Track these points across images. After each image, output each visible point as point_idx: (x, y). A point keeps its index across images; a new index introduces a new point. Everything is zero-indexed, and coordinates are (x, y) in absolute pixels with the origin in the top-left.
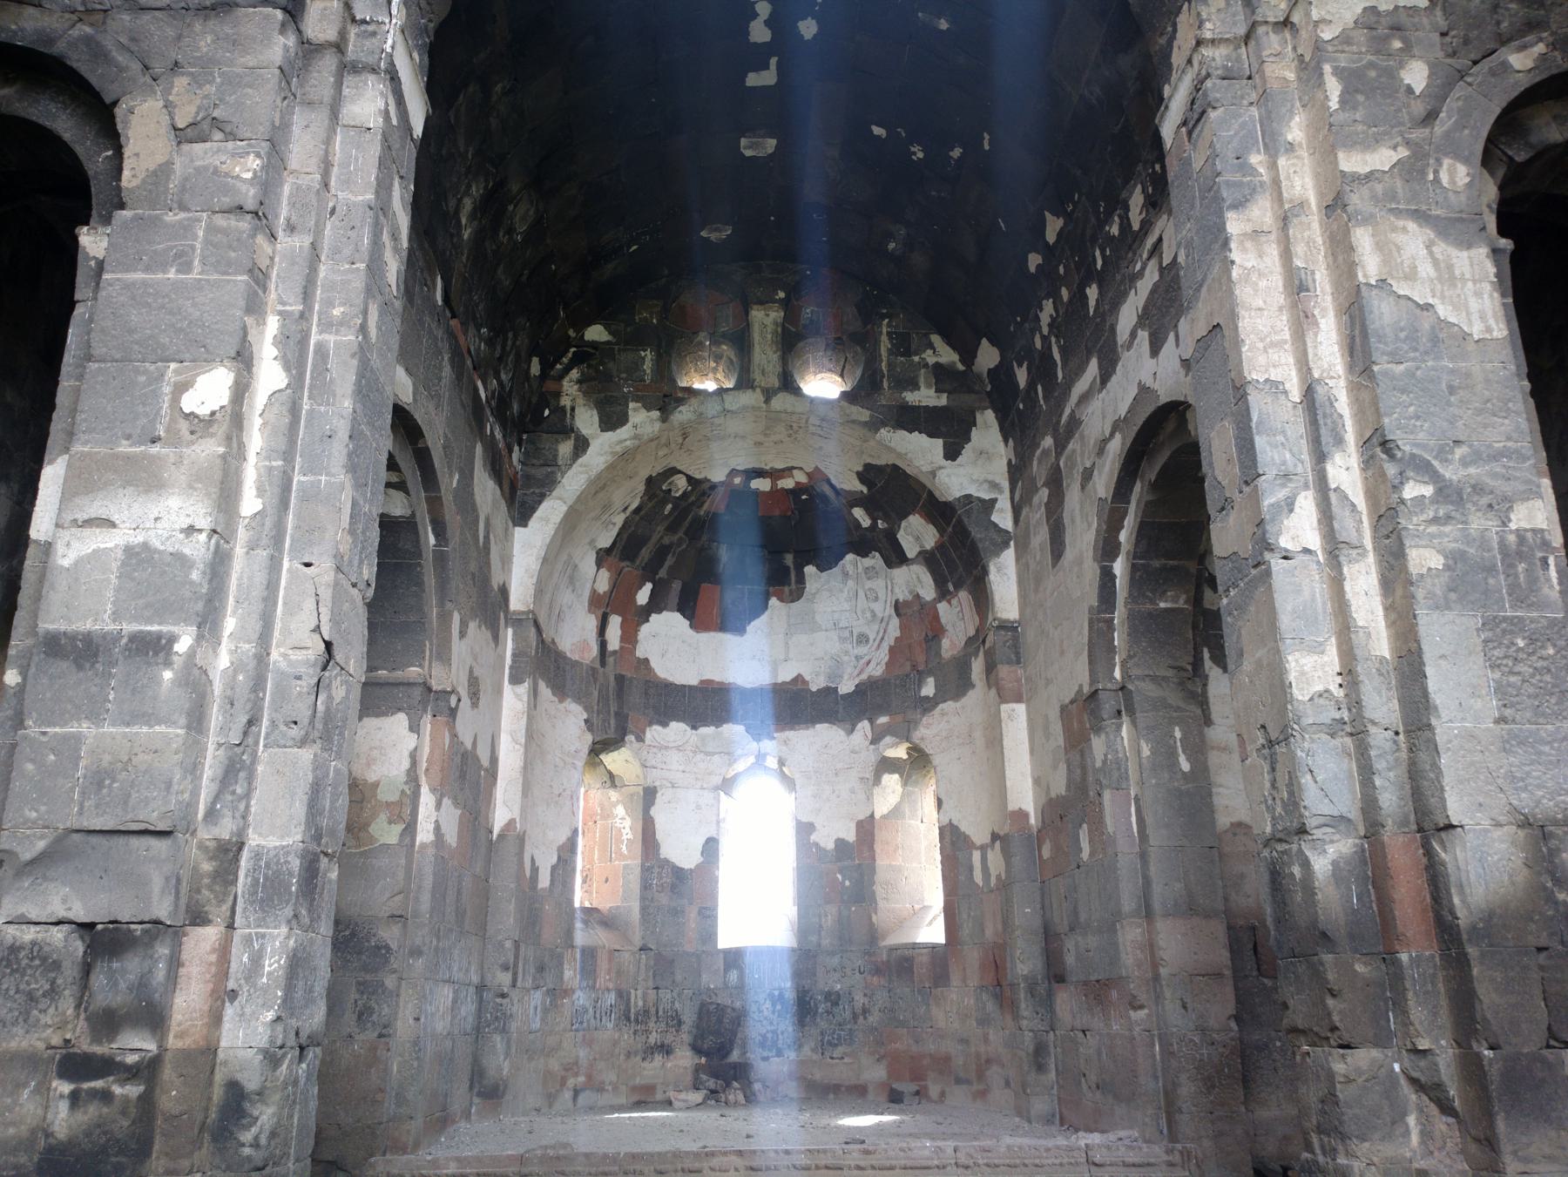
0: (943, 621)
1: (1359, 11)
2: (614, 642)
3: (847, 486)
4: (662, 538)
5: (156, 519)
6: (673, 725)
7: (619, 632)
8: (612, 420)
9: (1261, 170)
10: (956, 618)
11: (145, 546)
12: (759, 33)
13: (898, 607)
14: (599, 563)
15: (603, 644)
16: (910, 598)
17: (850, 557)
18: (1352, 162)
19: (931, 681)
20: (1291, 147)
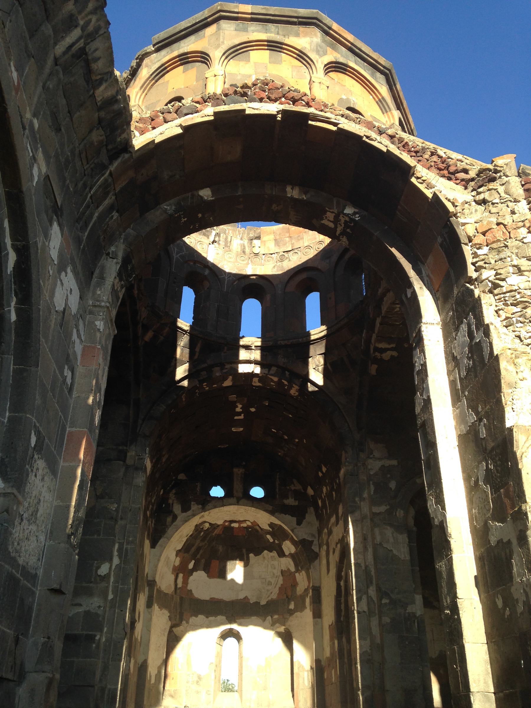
0: (297, 580)
1: (380, 466)
2: (180, 585)
3: (265, 528)
4: (199, 544)
5: (92, 604)
6: (200, 616)
7: (182, 580)
8: (185, 508)
9: (359, 503)
10: (301, 578)
11: (89, 611)
12: (238, 409)
13: (282, 572)
14: (177, 556)
15: (176, 585)
16: (286, 570)
17: (266, 552)
18: (376, 510)
19: (293, 603)
20: (364, 499)
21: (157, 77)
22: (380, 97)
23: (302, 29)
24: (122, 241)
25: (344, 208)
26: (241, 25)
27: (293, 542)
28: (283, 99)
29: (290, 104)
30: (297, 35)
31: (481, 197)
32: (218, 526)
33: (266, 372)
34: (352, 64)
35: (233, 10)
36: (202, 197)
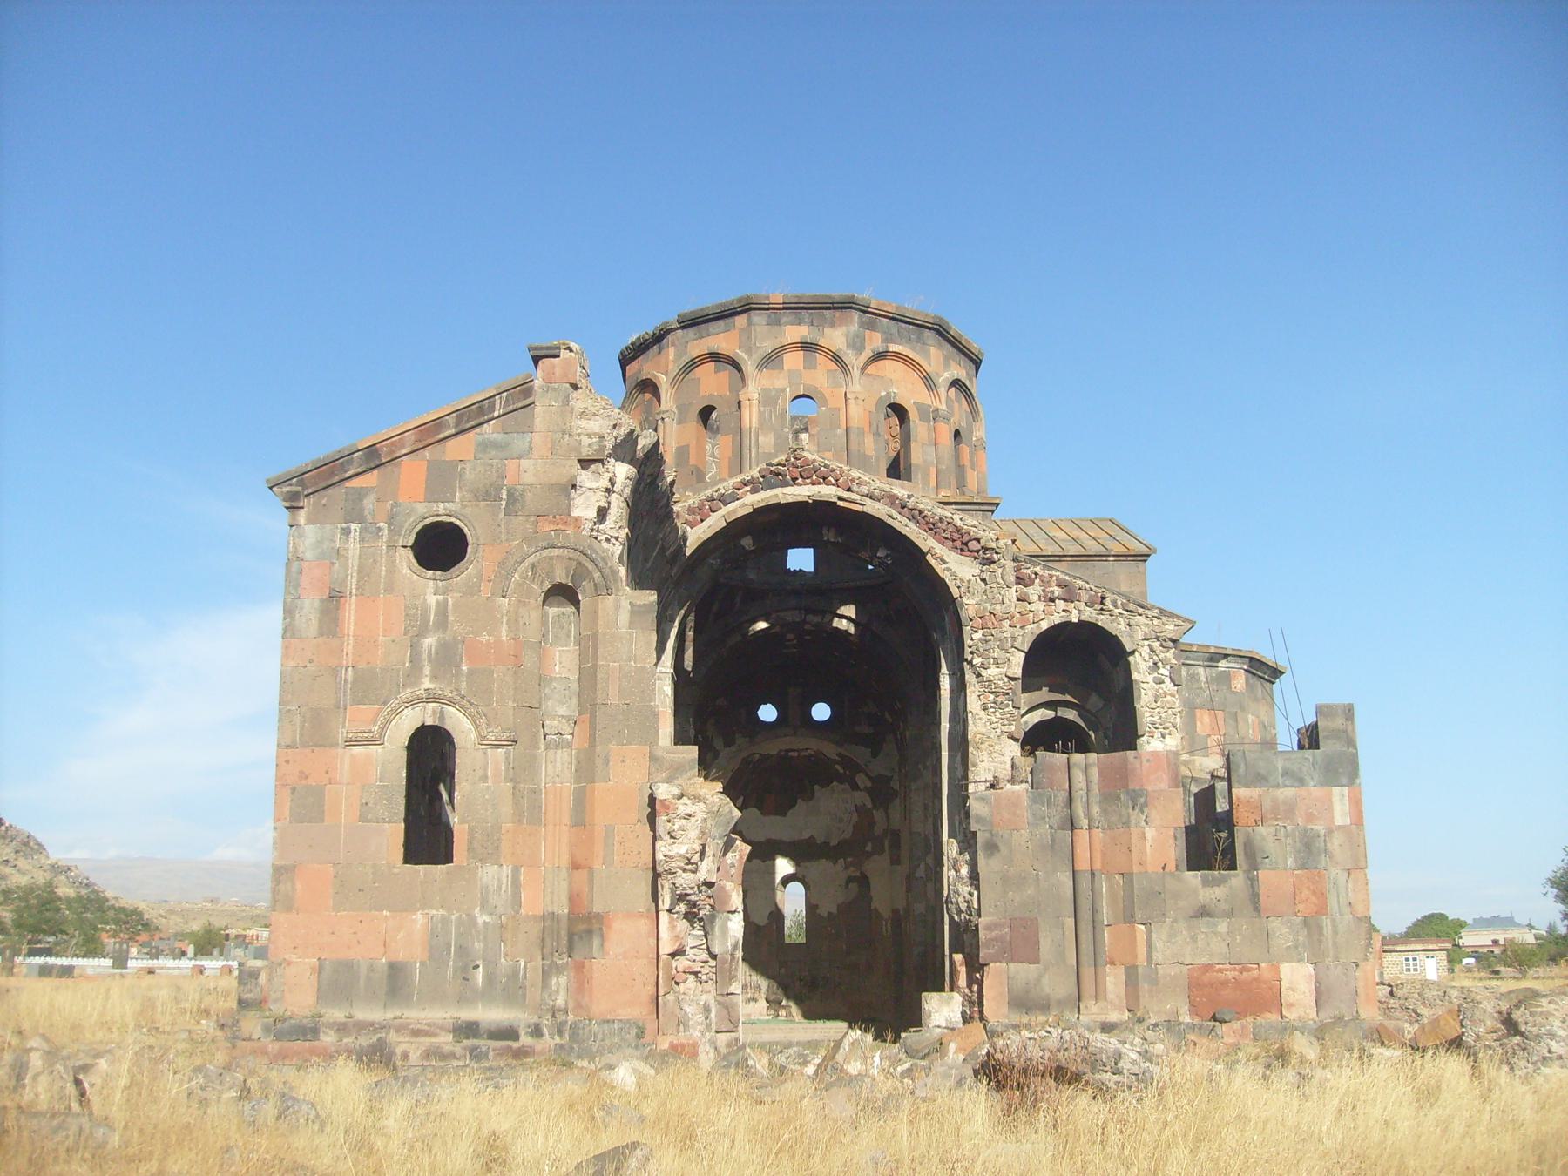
19: (870, 844)
21: (686, 372)
22: (925, 374)
23: (838, 313)
24: (676, 603)
25: (877, 551)
26: (773, 316)
27: (867, 775)
28: (814, 477)
29: (819, 483)
30: (833, 325)
31: (985, 576)
32: (772, 756)
33: (820, 620)
34: (893, 348)
35: (763, 302)
36: (744, 548)
